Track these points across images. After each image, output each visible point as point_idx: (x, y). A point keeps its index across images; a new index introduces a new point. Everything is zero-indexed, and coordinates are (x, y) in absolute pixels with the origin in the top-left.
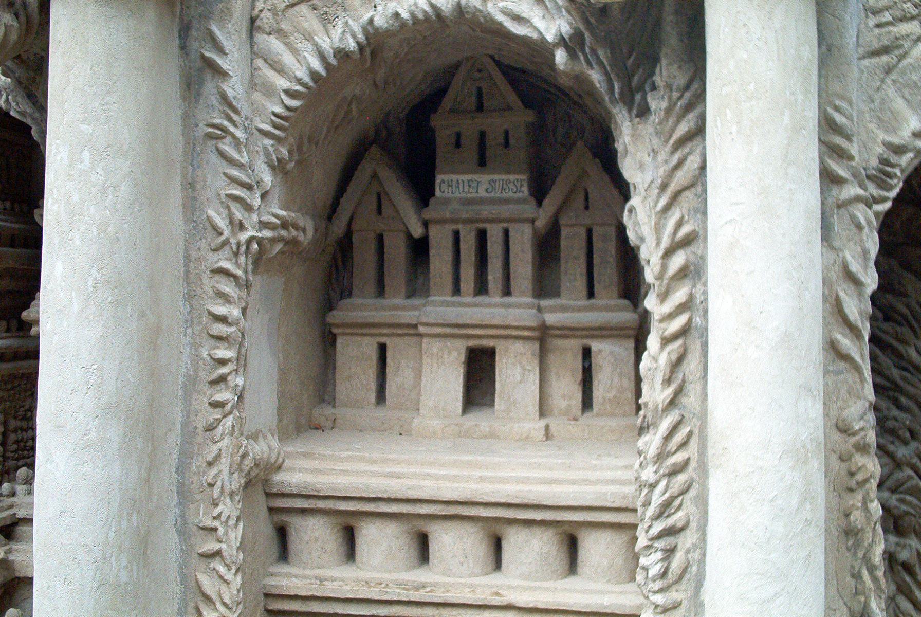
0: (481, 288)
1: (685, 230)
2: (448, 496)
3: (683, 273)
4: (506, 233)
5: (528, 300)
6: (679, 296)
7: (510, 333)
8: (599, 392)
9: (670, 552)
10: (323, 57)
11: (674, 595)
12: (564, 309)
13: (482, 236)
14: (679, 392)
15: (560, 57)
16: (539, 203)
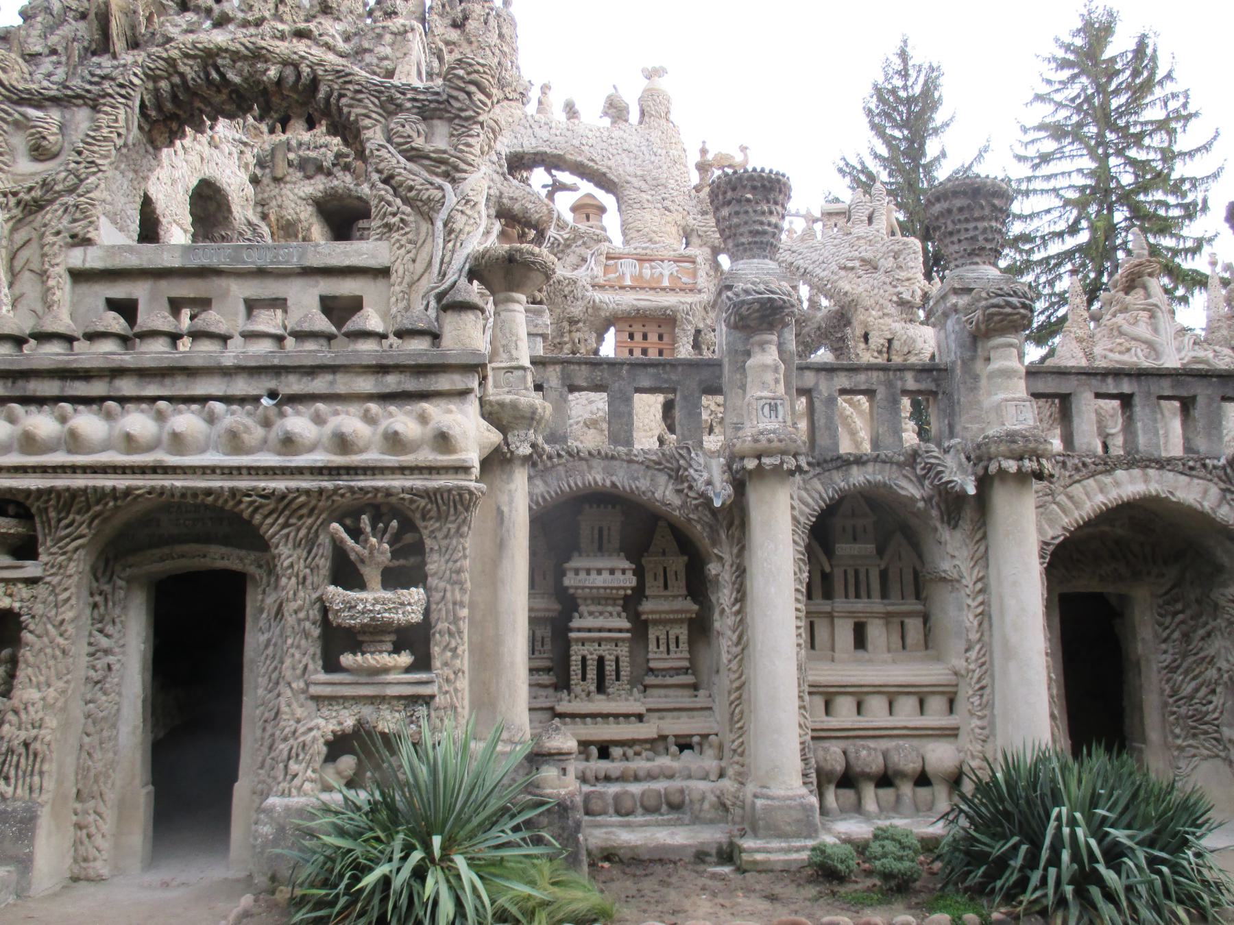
0: (857, 596)
1: (981, 575)
2: (877, 683)
3: (981, 591)
4: (867, 571)
5: (879, 600)
6: (980, 599)
7: (874, 615)
8: (909, 641)
9: (981, 696)
10: (824, 501)
11: (985, 712)
12: (893, 604)
13: (857, 573)
14: (982, 635)
15: (921, 504)
16: (881, 558)
